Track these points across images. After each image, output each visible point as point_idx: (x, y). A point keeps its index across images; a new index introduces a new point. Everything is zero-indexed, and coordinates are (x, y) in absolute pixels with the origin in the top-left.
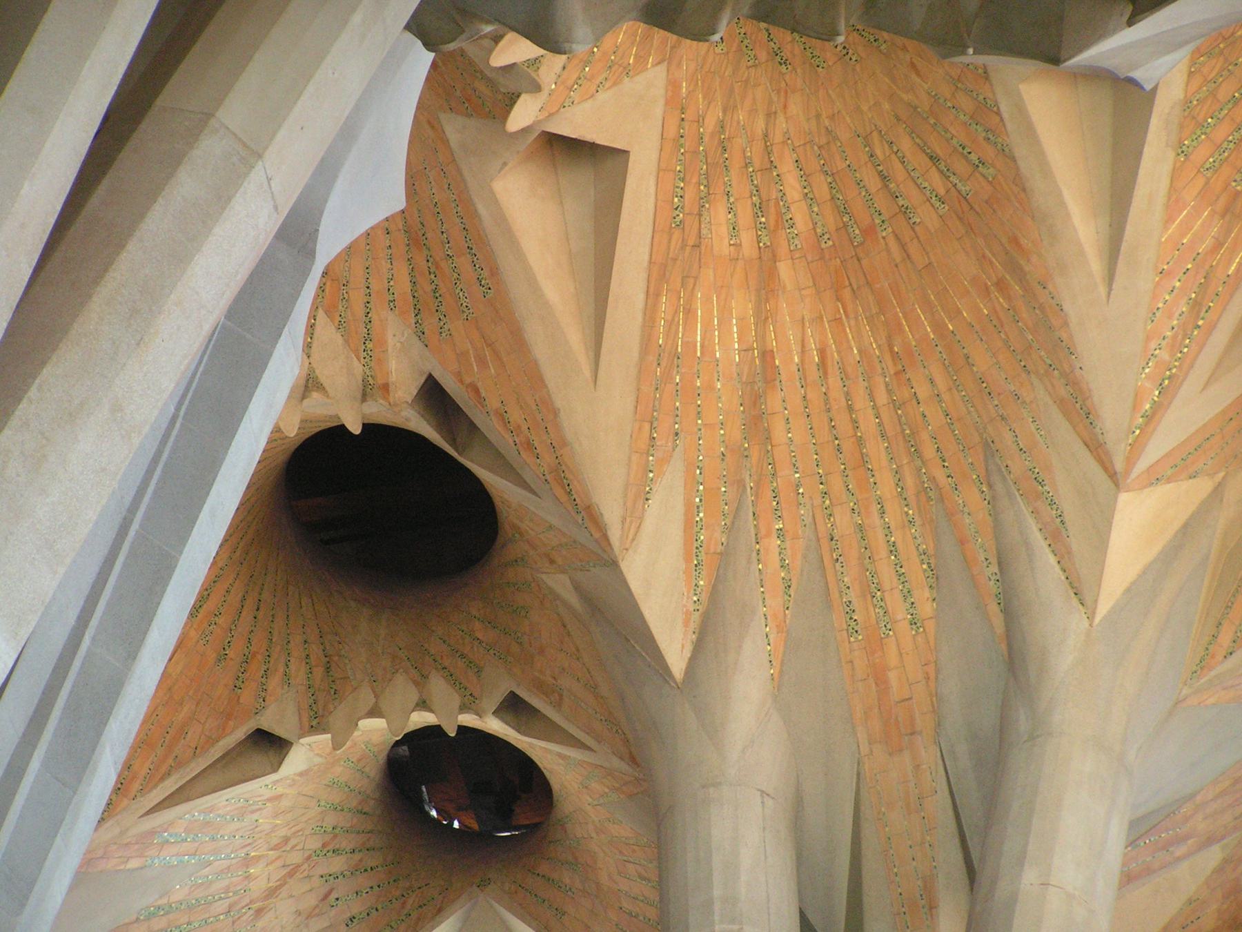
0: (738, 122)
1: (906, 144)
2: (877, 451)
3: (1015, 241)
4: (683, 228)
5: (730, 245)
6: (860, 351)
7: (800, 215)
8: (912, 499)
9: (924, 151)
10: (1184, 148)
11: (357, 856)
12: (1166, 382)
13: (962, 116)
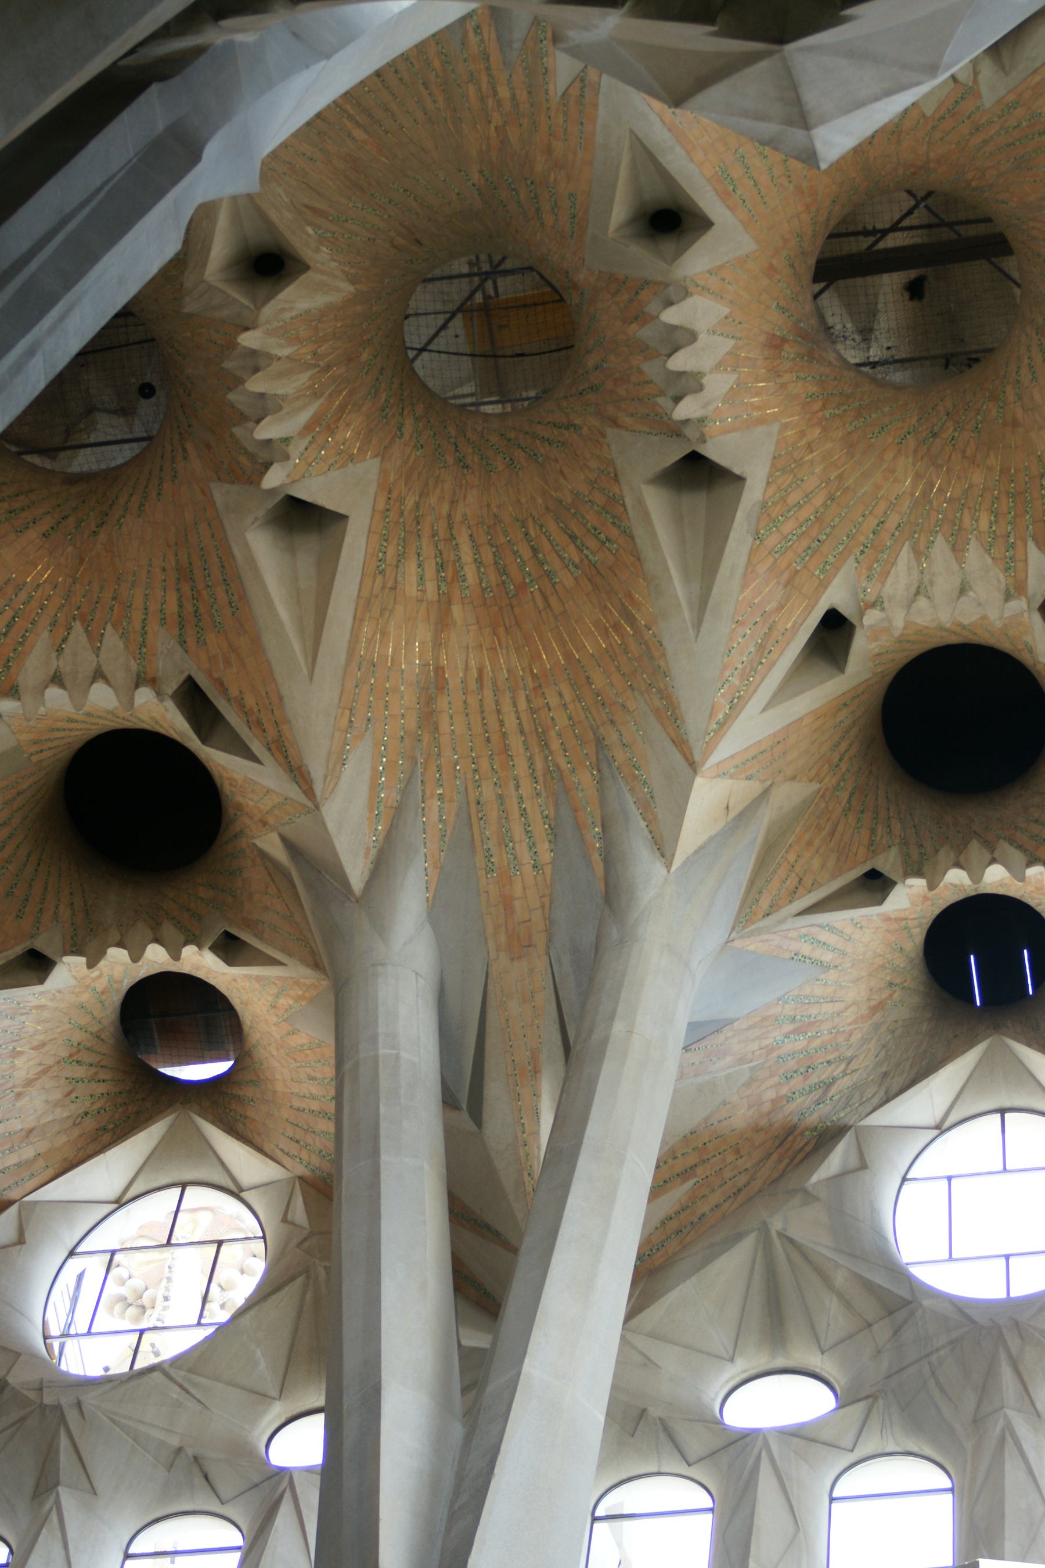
0: (430, 504)
1: (552, 526)
2: (516, 742)
3: (629, 596)
4: (384, 575)
5: (418, 590)
6: (508, 671)
7: (470, 573)
8: (541, 779)
9: (566, 532)
10: (760, 535)
11: (93, 1070)
12: (736, 700)
13: (596, 508)
